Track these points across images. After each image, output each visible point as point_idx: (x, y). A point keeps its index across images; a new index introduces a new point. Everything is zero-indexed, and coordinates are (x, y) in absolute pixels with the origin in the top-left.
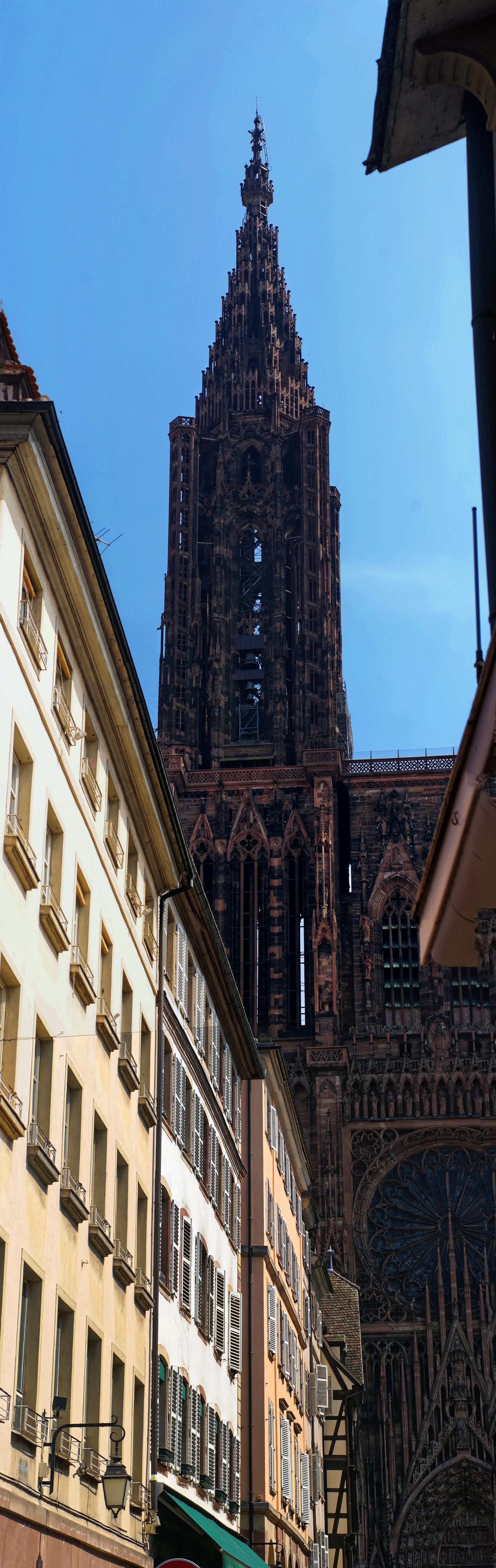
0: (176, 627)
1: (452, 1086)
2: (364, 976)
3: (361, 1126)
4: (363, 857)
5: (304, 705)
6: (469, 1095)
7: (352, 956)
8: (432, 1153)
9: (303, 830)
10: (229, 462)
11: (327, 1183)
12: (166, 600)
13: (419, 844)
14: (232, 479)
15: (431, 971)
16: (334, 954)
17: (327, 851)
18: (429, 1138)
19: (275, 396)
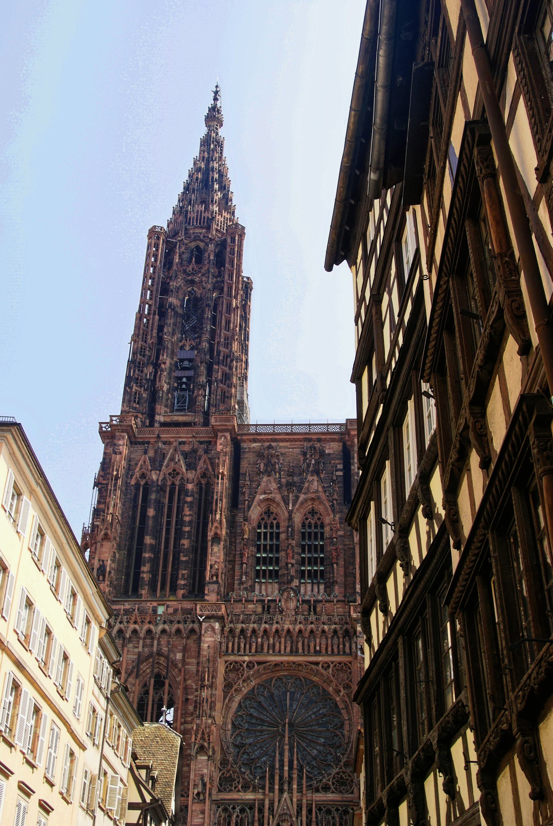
0: (140, 343)
1: (295, 634)
2: (242, 561)
3: (232, 658)
4: (247, 485)
5: (217, 392)
6: (306, 640)
7: (235, 548)
8: (279, 679)
9: (209, 467)
10: (183, 253)
11: (203, 693)
12: (135, 327)
13: (284, 478)
14: (183, 262)
15: (287, 559)
16: (222, 543)
17: (222, 479)
19: (213, 218)
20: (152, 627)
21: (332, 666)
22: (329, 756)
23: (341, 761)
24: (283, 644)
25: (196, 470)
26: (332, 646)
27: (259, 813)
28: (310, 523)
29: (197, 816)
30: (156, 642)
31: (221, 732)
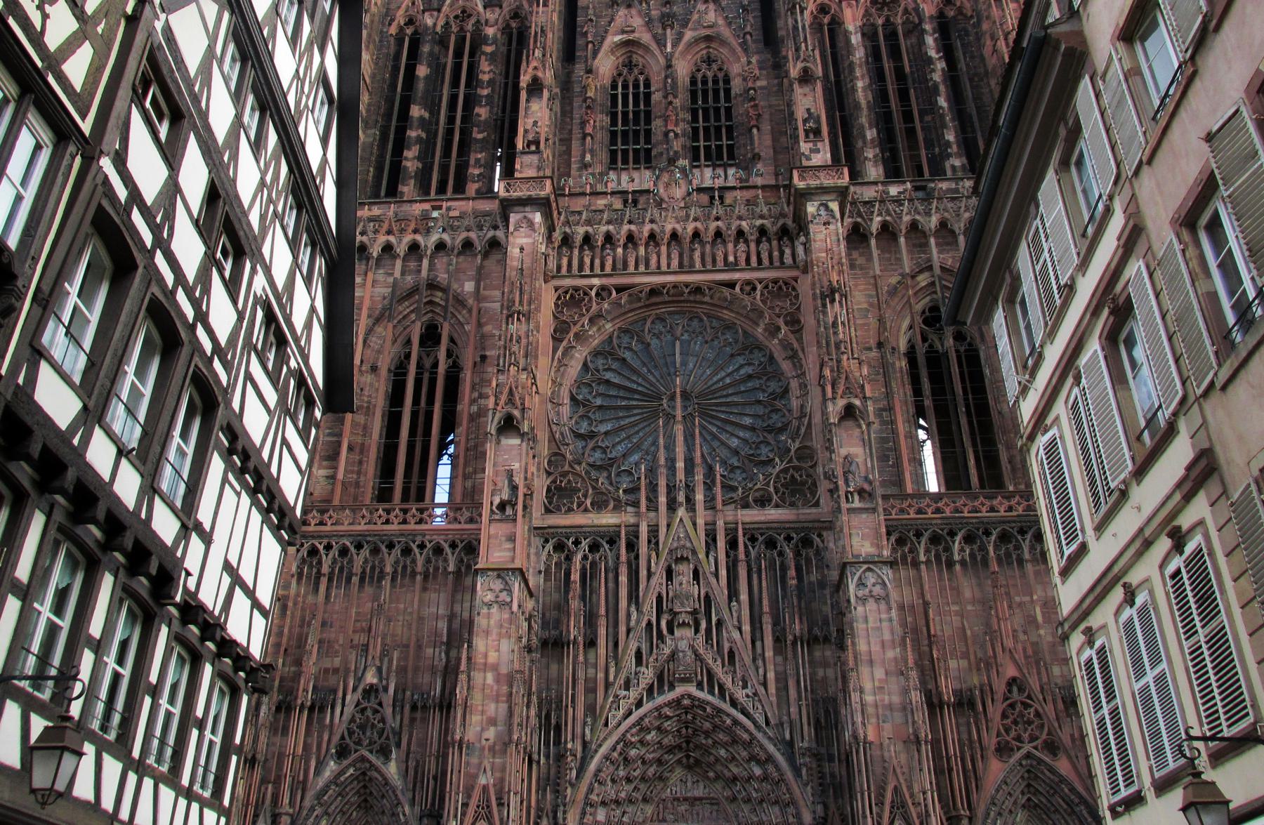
3: (568, 282)
4: (591, 20)
7: (572, 119)
11: (510, 326)
13: (656, 9)
15: (666, 126)
18: (654, 300)
20: (419, 238)
21: (759, 287)
22: (762, 446)
23: (790, 450)
24: (665, 256)
25: (501, 7)
26: (759, 254)
27: (627, 552)
28: (704, 76)
29: (500, 545)
30: (425, 262)
31: (549, 406)
